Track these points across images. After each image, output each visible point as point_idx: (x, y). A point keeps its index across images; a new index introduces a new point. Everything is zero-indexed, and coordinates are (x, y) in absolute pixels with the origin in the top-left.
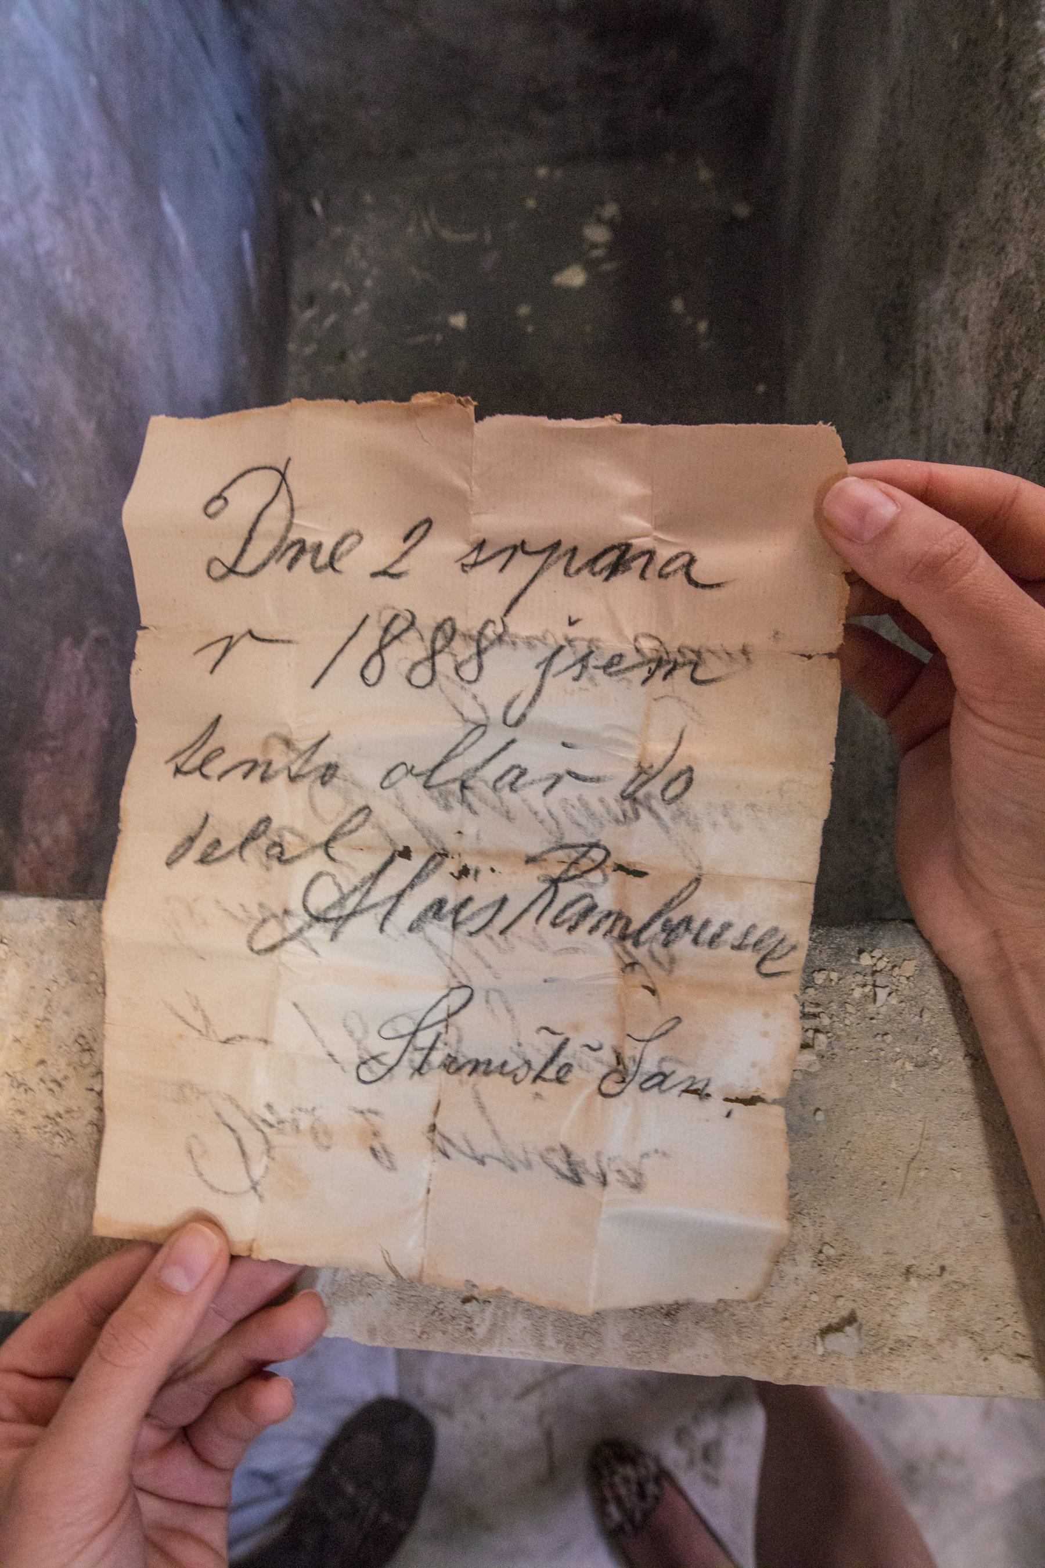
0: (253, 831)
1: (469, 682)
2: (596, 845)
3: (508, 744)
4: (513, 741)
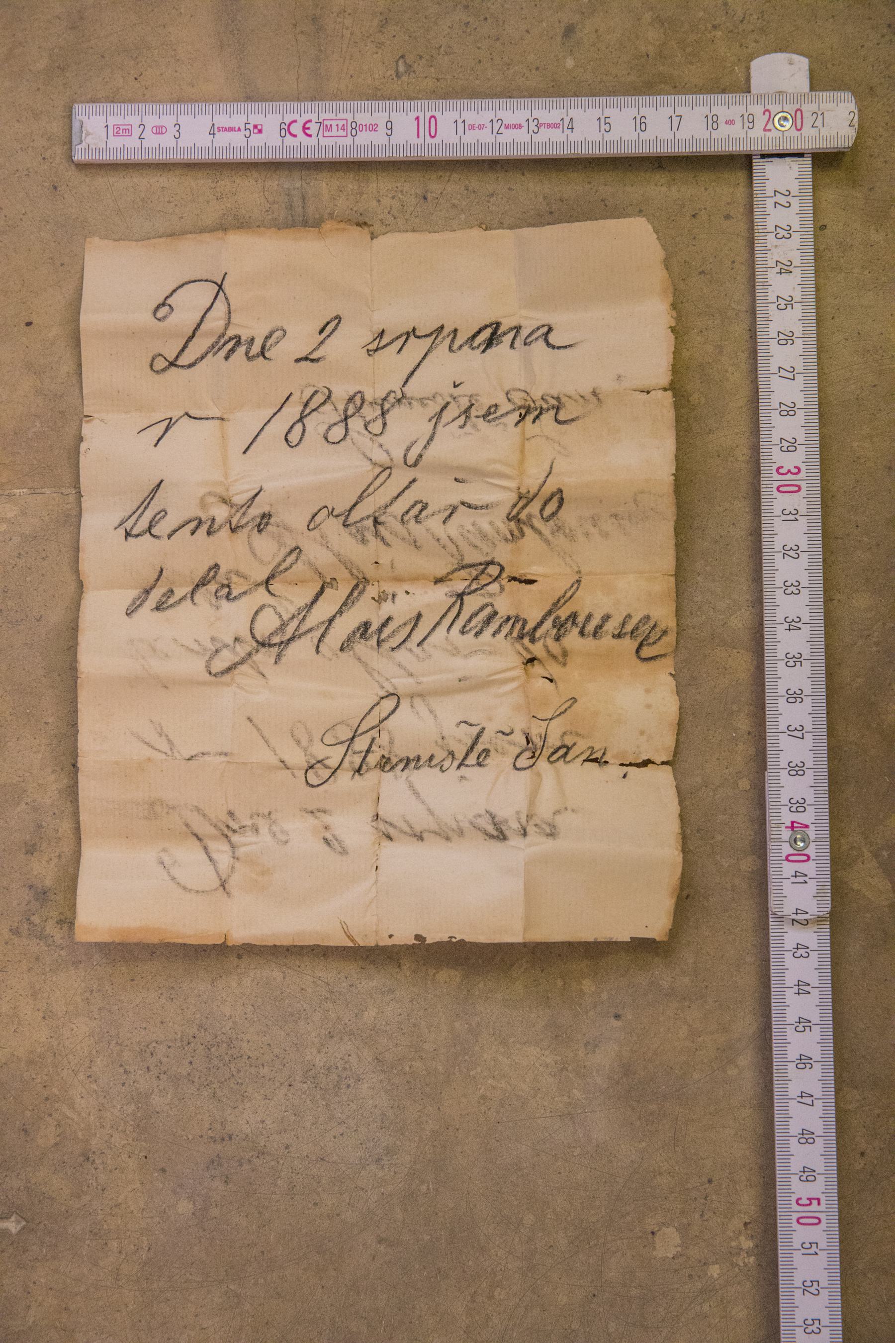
0: (204, 578)
1: (376, 435)
2: (492, 563)
3: (410, 483)
4: (414, 480)
